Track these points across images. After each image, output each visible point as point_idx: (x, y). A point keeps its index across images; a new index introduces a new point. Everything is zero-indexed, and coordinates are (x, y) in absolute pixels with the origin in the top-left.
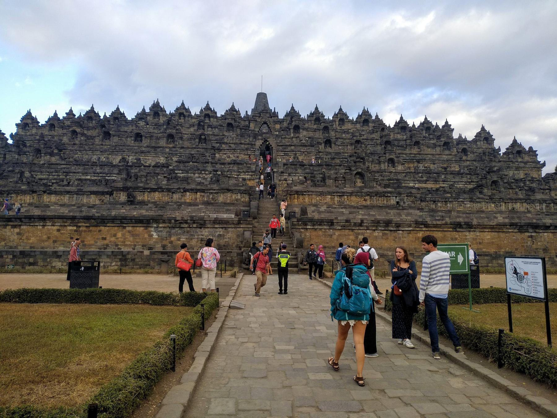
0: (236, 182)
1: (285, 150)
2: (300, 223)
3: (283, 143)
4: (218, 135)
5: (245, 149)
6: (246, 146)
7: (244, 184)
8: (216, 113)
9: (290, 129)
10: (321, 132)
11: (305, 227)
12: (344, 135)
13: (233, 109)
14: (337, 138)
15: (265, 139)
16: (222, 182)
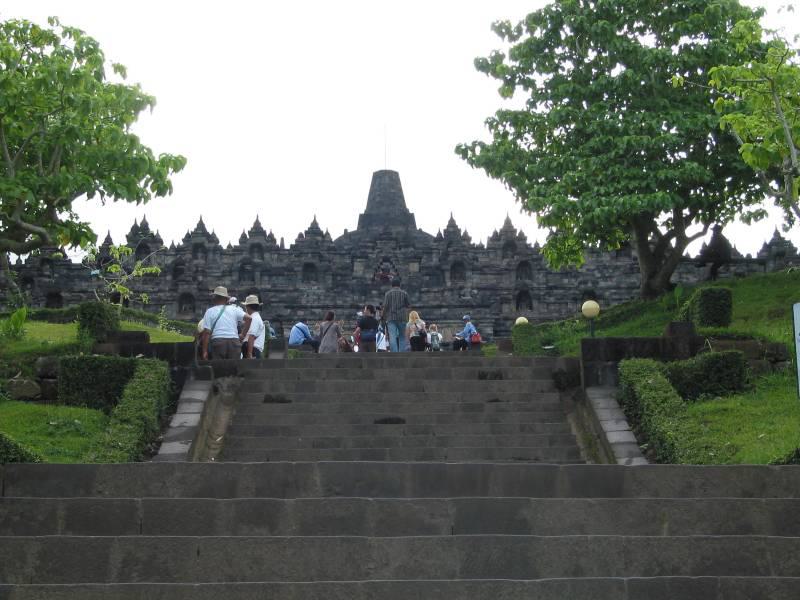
4: (283, 291)
6: (346, 312)
9: (443, 271)
10: (513, 275)
12: (566, 281)
13: (314, 229)
14: (551, 288)
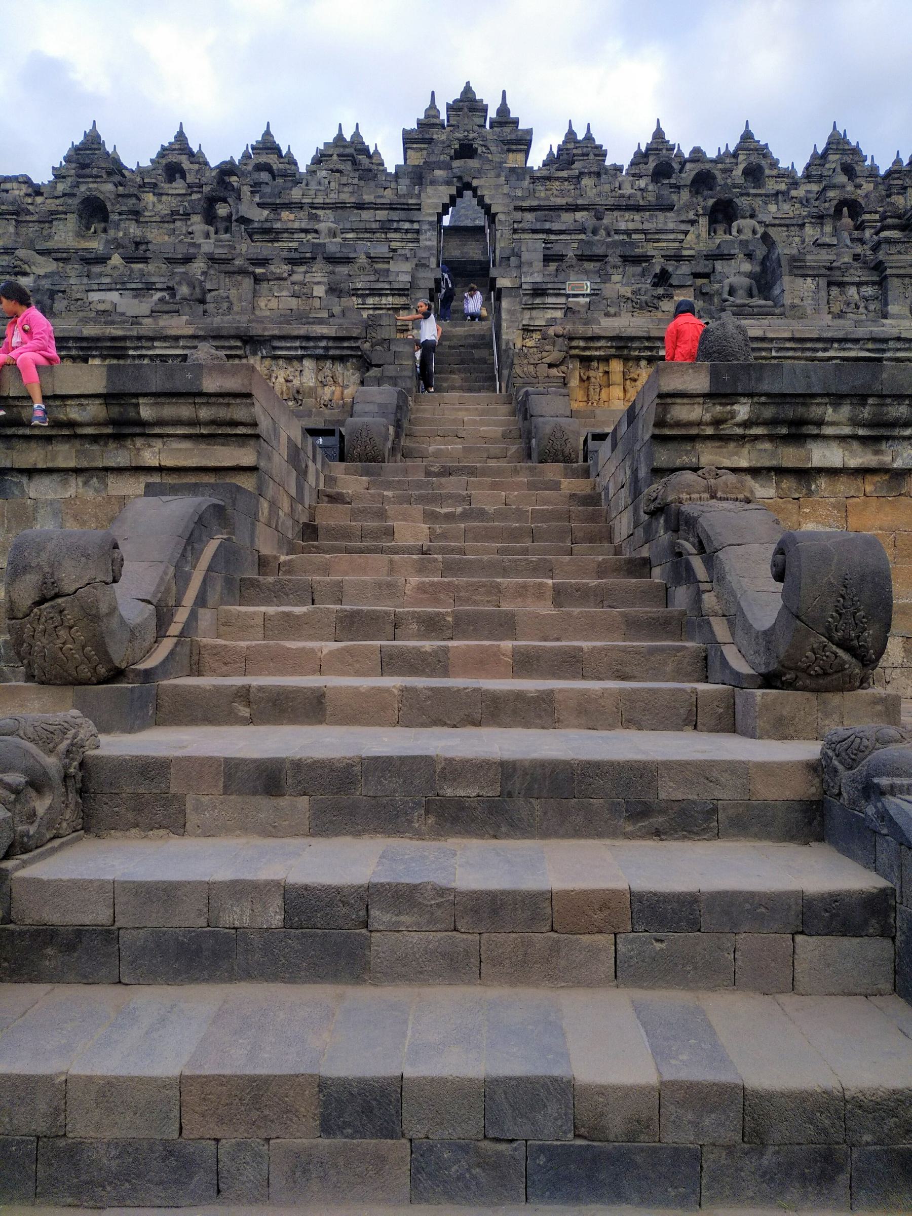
0: (293, 303)
1: (547, 226)
2: (743, 411)
3: (539, 198)
5: (375, 226)
6: (382, 215)
7: (337, 310)
8: (296, 164)
11: (789, 456)
15: (460, 178)
16: (216, 301)
